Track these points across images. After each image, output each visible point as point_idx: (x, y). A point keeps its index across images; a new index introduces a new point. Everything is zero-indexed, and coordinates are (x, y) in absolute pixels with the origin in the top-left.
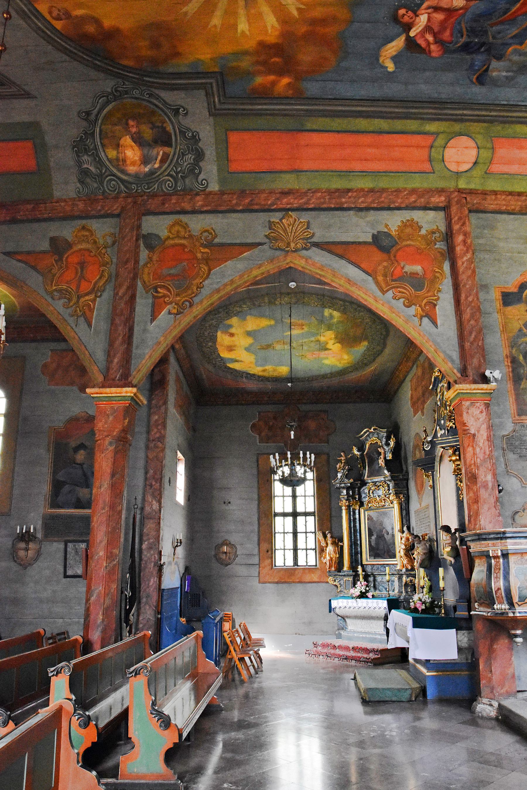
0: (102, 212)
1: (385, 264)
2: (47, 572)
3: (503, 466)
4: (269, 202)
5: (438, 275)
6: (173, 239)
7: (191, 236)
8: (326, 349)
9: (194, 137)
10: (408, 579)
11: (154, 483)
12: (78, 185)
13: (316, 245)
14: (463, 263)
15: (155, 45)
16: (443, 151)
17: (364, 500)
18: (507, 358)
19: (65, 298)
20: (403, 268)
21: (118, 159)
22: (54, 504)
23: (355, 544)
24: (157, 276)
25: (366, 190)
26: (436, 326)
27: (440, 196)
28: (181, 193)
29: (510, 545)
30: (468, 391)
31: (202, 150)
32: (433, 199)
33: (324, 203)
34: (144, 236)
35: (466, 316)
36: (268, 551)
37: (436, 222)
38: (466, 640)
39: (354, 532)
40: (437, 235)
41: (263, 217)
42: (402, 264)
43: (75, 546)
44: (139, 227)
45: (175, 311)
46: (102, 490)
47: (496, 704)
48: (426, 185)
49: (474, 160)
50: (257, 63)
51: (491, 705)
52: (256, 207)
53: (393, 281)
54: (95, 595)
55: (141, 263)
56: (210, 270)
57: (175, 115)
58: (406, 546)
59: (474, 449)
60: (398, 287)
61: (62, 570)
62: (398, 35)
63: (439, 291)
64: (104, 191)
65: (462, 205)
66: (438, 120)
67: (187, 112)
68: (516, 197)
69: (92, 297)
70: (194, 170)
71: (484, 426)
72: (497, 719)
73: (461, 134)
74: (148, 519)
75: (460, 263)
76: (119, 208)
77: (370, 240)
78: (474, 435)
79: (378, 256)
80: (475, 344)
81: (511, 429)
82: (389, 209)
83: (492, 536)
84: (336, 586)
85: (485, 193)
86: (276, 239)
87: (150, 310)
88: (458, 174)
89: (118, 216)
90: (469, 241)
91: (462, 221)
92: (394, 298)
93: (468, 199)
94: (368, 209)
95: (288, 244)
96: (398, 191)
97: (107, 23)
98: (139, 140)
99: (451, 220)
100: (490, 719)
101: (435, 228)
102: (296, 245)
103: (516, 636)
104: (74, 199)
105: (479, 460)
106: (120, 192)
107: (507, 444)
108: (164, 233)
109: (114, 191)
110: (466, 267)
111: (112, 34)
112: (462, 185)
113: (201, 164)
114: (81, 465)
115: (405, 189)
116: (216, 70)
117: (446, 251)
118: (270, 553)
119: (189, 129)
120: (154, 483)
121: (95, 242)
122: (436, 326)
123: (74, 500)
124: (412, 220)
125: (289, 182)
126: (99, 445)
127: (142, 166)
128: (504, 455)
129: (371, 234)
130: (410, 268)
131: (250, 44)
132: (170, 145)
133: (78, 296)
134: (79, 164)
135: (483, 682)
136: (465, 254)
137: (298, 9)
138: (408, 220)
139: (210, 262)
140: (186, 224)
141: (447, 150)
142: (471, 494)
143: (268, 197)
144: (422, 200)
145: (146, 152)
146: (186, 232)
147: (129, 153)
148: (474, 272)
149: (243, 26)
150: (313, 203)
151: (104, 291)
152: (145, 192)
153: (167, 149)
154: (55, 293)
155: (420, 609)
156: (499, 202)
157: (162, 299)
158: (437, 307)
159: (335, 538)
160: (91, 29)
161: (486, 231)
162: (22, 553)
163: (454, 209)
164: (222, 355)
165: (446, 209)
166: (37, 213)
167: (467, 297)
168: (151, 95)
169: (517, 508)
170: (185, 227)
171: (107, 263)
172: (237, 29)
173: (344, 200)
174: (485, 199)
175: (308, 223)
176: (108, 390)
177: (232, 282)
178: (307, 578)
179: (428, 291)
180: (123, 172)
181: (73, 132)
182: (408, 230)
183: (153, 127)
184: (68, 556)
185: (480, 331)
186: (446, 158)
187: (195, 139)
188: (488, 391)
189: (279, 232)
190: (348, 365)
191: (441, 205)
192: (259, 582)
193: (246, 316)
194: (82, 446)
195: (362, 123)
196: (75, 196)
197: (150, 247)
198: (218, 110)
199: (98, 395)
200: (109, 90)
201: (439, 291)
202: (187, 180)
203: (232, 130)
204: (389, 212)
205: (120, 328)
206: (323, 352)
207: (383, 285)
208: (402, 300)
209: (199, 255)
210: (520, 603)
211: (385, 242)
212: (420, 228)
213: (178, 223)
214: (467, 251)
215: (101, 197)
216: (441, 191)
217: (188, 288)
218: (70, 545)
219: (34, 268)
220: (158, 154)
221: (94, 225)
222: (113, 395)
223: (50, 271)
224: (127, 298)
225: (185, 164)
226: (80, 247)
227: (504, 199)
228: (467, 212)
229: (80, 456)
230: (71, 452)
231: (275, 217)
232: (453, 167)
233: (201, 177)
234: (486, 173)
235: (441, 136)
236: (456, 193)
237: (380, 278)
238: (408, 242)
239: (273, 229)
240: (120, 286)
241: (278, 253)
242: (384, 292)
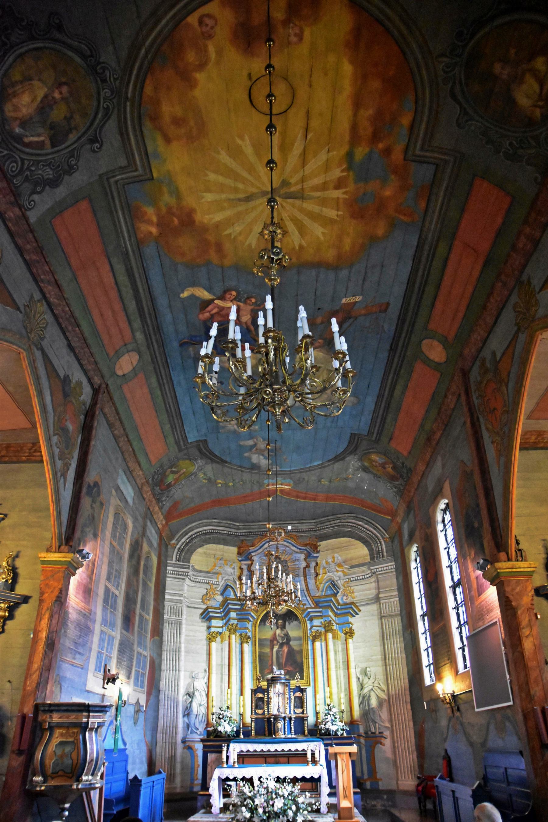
9: (71, 167)
15: (178, 122)
32: (96, 378)
49: (126, 372)
50: (169, 209)
57: (90, 140)
62: (214, 295)
66: (146, 336)
67: (97, 152)
73: (139, 353)
97: (200, 76)
98: (45, 107)
111: (186, 78)
113: (47, 188)
116: (155, 175)
127: (18, 122)
131: (190, 201)
132: (53, 146)
137: (230, 234)
141: (127, 355)
147: (25, 99)
149: (209, 197)
160: (191, 57)
168: (107, 109)
172: (205, 192)
174: (108, 402)
183: (68, 119)
187: (70, 170)
200: (101, 60)
202: (26, 185)
220: (39, 135)
225: (40, 172)
233: (36, 197)
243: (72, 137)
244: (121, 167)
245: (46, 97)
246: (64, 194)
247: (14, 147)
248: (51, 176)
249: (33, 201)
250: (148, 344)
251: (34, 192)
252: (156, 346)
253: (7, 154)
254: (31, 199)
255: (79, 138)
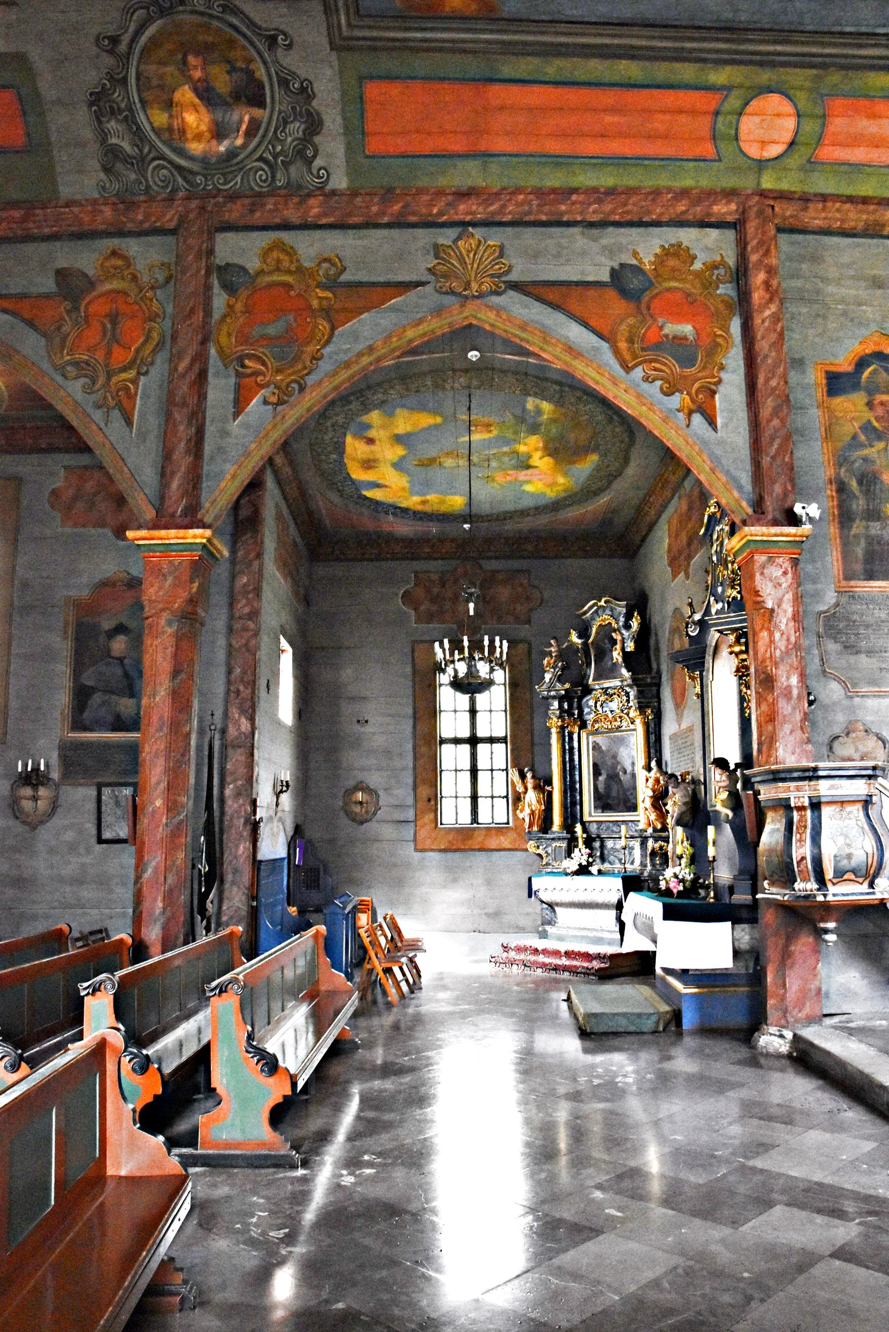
0: (146, 225)
1: (631, 321)
2: (69, 836)
3: (817, 661)
4: (435, 211)
5: (719, 340)
6: (270, 273)
7: (300, 270)
8: (529, 467)
9: (303, 90)
10: (657, 845)
11: (242, 688)
12: (102, 175)
13: (516, 286)
14: (763, 321)
16: (738, 120)
17: (587, 717)
18: (831, 483)
19: (86, 376)
20: (661, 328)
21: (170, 129)
22: (78, 725)
23: (571, 789)
24: (244, 338)
25: (602, 190)
26: (715, 429)
27: (728, 203)
28: (283, 192)
29: (824, 788)
30: (765, 538)
31: (318, 114)
32: (716, 208)
33: (530, 213)
34: (219, 268)
35: (765, 412)
36: (429, 800)
37: (721, 248)
38: (747, 937)
39: (570, 769)
40: (722, 271)
41: (424, 237)
42: (660, 321)
43: (113, 791)
44: (211, 252)
45: (274, 399)
46: (157, 699)
47: (789, 1035)
48: (705, 182)
49: (788, 137)
51: (781, 1036)
52: (413, 219)
53: (643, 349)
54: (150, 871)
55: (216, 316)
56: (333, 329)
58: (654, 791)
59: (771, 634)
60: (651, 361)
61: (94, 831)
63: (722, 368)
64: (148, 187)
65: (769, 218)
67: (291, 42)
68: (860, 206)
69: (132, 374)
70: (304, 152)
71: (789, 596)
72: (789, 1056)
74: (234, 747)
75: (757, 321)
76: (176, 218)
77: (605, 277)
78: (772, 610)
79: (617, 306)
80: (779, 461)
81: (834, 601)
82: (640, 224)
83: (796, 775)
84: (540, 855)
85: (805, 199)
86: (446, 276)
87: (231, 397)
88: (761, 165)
89: (173, 232)
90: (774, 283)
91: (765, 248)
92: (646, 379)
93: (777, 209)
94: (603, 224)
95: (467, 286)
96: (656, 193)
98: (206, 95)
99: (746, 244)
100: (779, 1056)
101: (719, 258)
102: (480, 286)
103: (826, 931)
104: (95, 202)
105: (778, 653)
106: (174, 191)
107: (825, 625)
108: (253, 264)
109: (167, 186)
110: (767, 329)
112: (767, 183)
114: (121, 660)
115: (669, 190)
117: (736, 299)
118: (433, 802)
119: (293, 74)
120: (242, 688)
121: (135, 278)
122: (715, 429)
123: (110, 718)
124: (680, 245)
125: (468, 174)
126: (151, 626)
128: (819, 644)
129: (608, 268)
130: (671, 328)
132: (261, 104)
133: (108, 372)
134: (103, 135)
135: (771, 1002)
136: (766, 306)
138: (672, 245)
139: (334, 317)
140: (291, 247)
141: (744, 119)
142: (764, 707)
143: (432, 200)
144: (699, 209)
145: (219, 115)
146: (292, 262)
147: (190, 118)
148: (781, 335)
150: (510, 213)
151: (152, 363)
152: (219, 190)
153: (258, 112)
154: (69, 368)
155: (675, 891)
156: (830, 215)
157: (253, 379)
158: (717, 396)
159: (540, 779)
161: (804, 266)
162: (27, 805)
163: (751, 227)
164: (354, 476)
165: (737, 225)
166: (31, 225)
167: (767, 380)
169: (837, 730)
170: (290, 252)
171: (157, 315)
173: (563, 208)
174: (806, 209)
175: (502, 247)
176: (163, 533)
177: (371, 349)
178: (493, 843)
179: (704, 368)
180: (181, 152)
181: (92, 77)
182: (672, 262)
184: (103, 808)
185: (788, 437)
186: (742, 135)
187: (306, 92)
188: (797, 539)
189: (450, 263)
190: (564, 495)
191: (730, 219)
192: (416, 850)
193: (395, 408)
194: (120, 629)
195: (596, 68)
196: (97, 196)
197: (230, 288)
198: (345, 39)
199: (147, 542)
201: (722, 368)
202: (293, 170)
203: (372, 78)
204: (641, 230)
205: (182, 428)
206: (524, 472)
207: (627, 356)
208: (658, 383)
209: (315, 303)
210: (835, 881)
211: (635, 283)
212: (694, 258)
213: (279, 246)
214: (771, 300)
215: (142, 198)
216: (730, 194)
217: (297, 359)
218: (106, 792)
219: (31, 324)
220: (241, 121)
221: (133, 247)
222: (172, 541)
223: (59, 329)
224: (192, 376)
225: (289, 139)
226: (108, 287)
227: (838, 210)
228: (773, 232)
229: (119, 645)
230: (102, 639)
231: (446, 237)
232: (754, 151)
233: (318, 162)
234: (809, 161)
235: (735, 93)
236: (757, 198)
237: (623, 345)
238: (674, 284)
239: (443, 259)
240: (180, 356)
241: (448, 300)
242: (628, 369)
243: (261, 73)
244: (325, 13)
245: (196, 90)
246: (339, 119)
247: (242, 161)
248: (303, 126)
249: (320, 169)
250: (761, 64)
251: (309, 162)
252: (779, 48)
253: (242, 179)
254: (315, 172)
255: (265, 63)
